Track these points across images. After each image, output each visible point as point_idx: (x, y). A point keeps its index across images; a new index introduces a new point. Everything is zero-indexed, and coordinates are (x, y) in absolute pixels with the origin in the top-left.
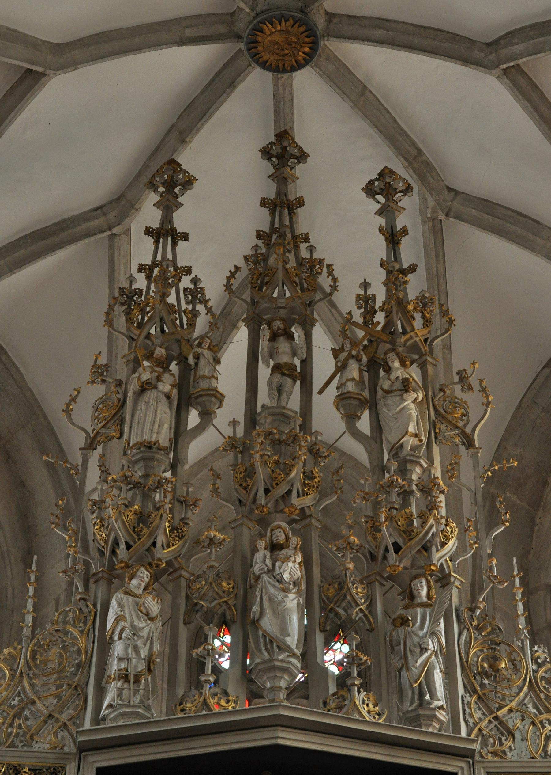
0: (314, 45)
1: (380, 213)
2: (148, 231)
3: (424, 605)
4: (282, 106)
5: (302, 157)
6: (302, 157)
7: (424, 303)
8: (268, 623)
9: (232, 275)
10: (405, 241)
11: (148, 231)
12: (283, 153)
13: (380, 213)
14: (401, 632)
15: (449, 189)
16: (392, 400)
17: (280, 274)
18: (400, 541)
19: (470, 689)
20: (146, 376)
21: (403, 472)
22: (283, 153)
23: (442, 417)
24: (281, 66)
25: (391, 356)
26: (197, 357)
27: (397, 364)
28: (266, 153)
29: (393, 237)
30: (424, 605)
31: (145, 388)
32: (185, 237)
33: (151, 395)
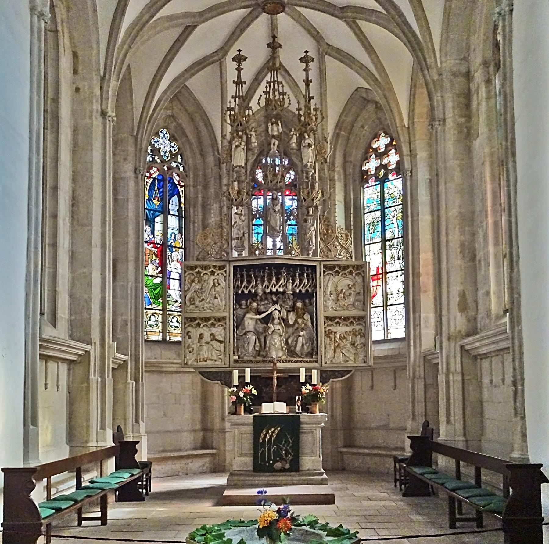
0: (284, 8)
1: (304, 70)
2: (234, 82)
3: (311, 216)
4: (273, 27)
5: (280, 46)
6: (280, 46)
7: (315, 110)
8: (272, 223)
9: (260, 98)
10: (311, 84)
11: (234, 82)
12: (274, 45)
13: (304, 70)
14: (305, 224)
15: (327, 44)
16: (306, 149)
17: (274, 102)
18: (306, 198)
19: (321, 239)
20: (237, 144)
21: (307, 174)
22: (274, 45)
23: (319, 153)
24: (273, 12)
25: (305, 134)
26: (251, 135)
27: (307, 137)
28: (269, 45)
29: (308, 82)
30: (311, 216)
31: (237, 147)
32: (245, 83)
33: (239, 149)
